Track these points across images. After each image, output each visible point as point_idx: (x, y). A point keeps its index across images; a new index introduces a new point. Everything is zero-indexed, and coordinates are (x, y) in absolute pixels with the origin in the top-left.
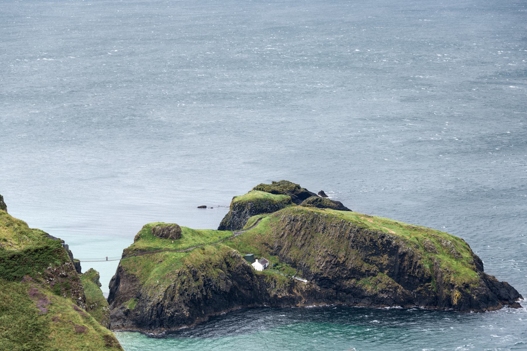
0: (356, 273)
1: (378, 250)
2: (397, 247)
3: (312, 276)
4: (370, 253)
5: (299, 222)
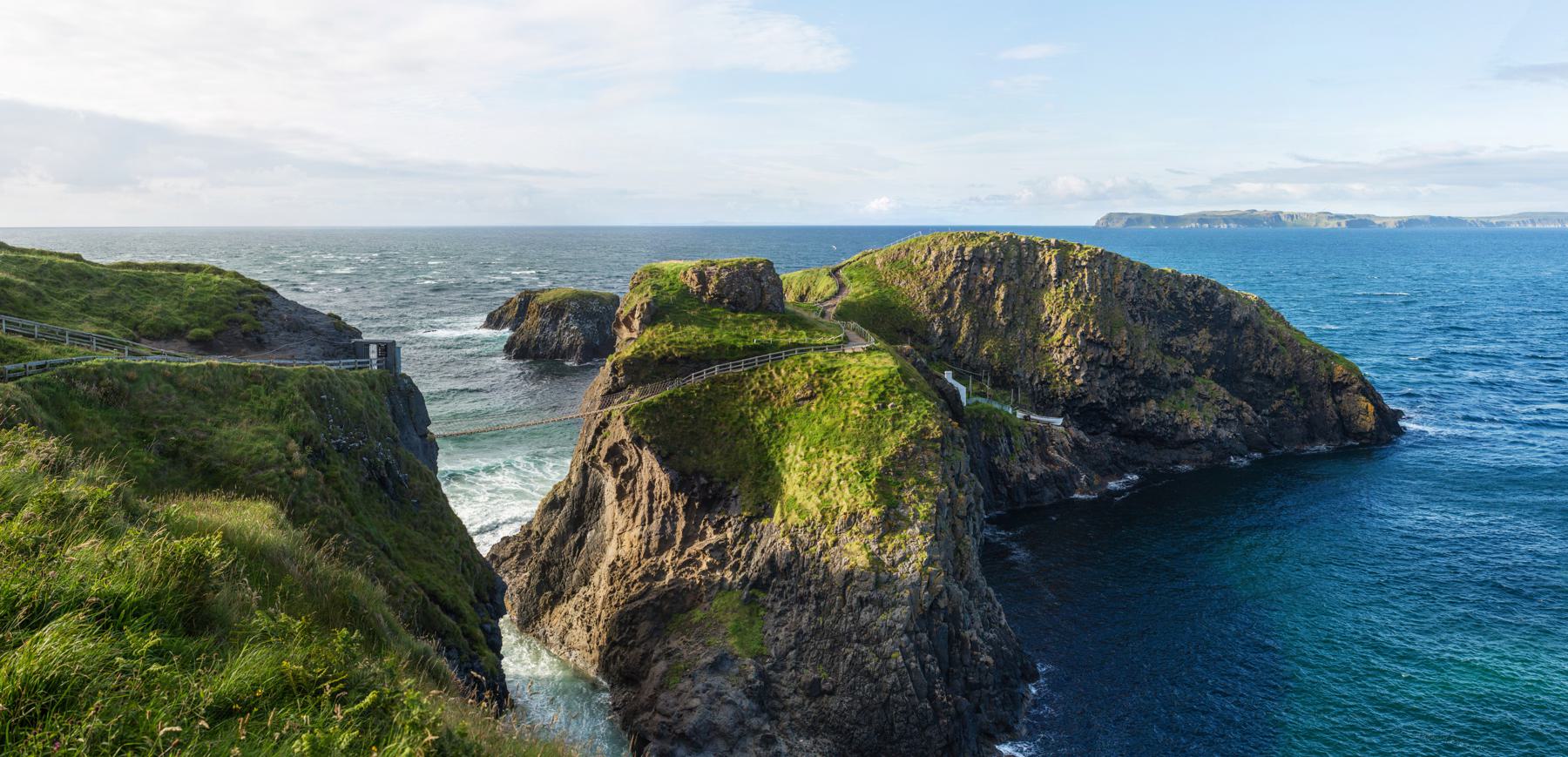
0: (1153, 383)
2: (1230, 306)
3: (1058, 407)
4: (1172, 328)
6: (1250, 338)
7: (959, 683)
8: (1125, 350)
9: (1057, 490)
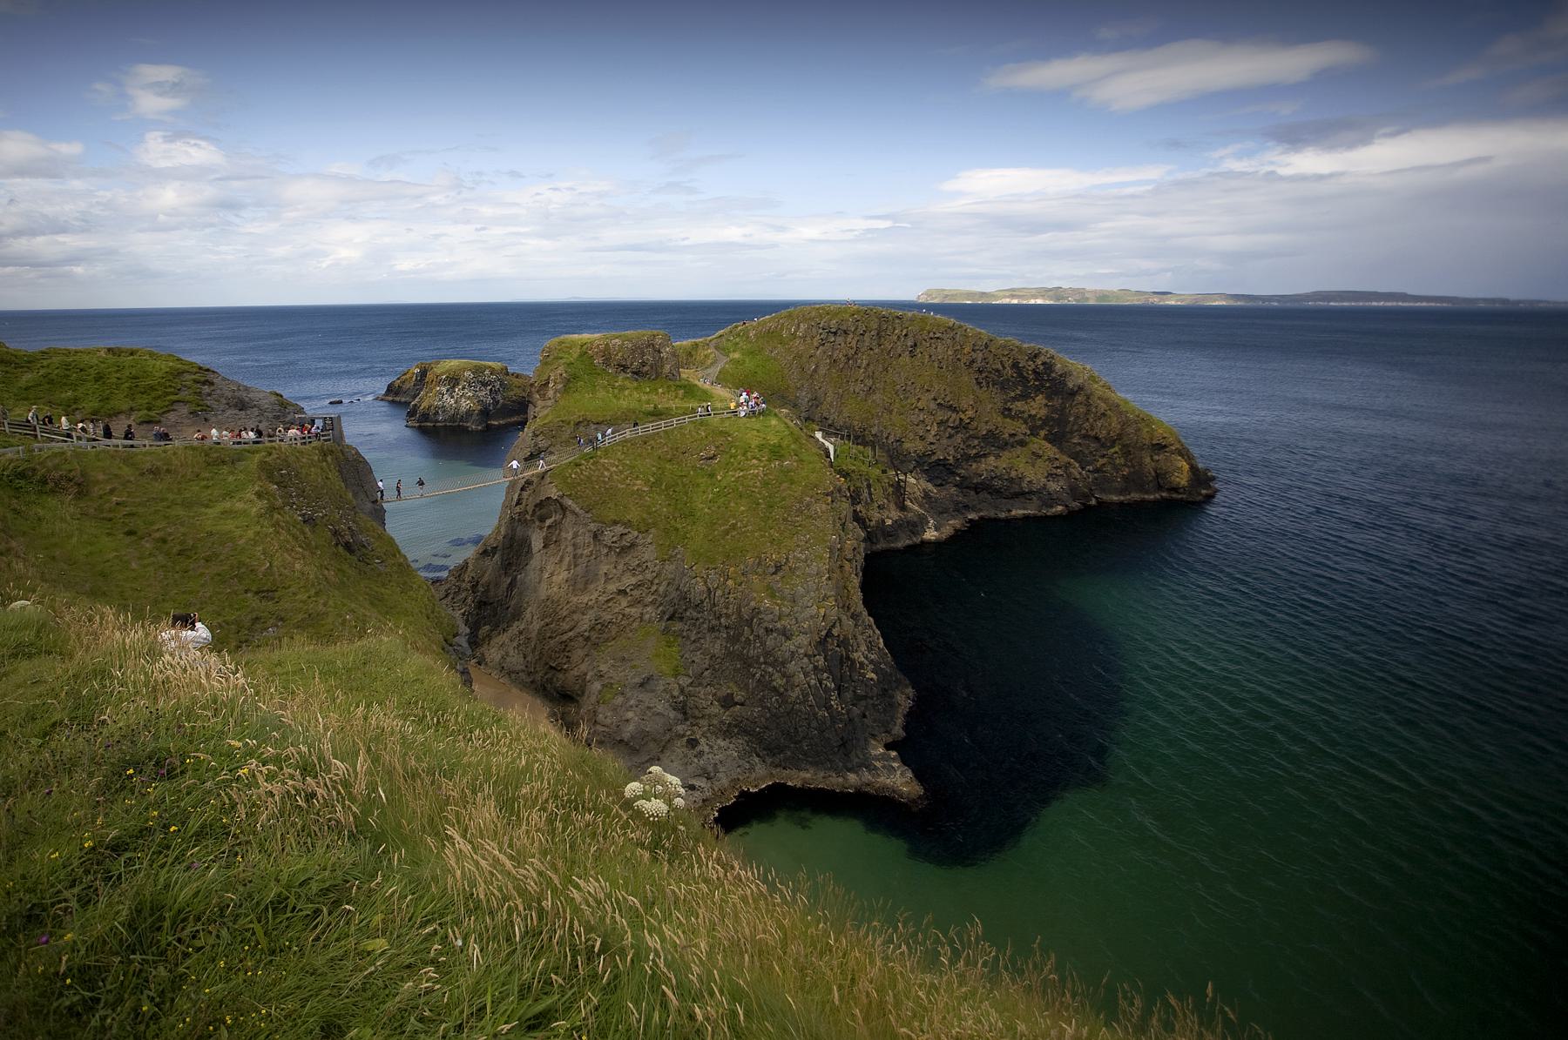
0: (995, 442)
1: (1028, 387)
4: (1013, 394)
5: (851, 336)
6: (1081, 403)
7: (848, 695)
8: (970, 413)
9: (909, 533)
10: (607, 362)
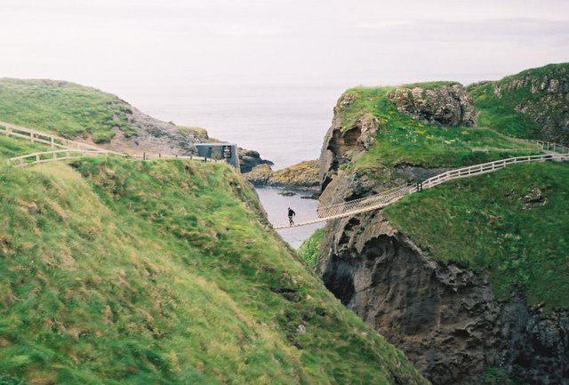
10: (410, 108)
